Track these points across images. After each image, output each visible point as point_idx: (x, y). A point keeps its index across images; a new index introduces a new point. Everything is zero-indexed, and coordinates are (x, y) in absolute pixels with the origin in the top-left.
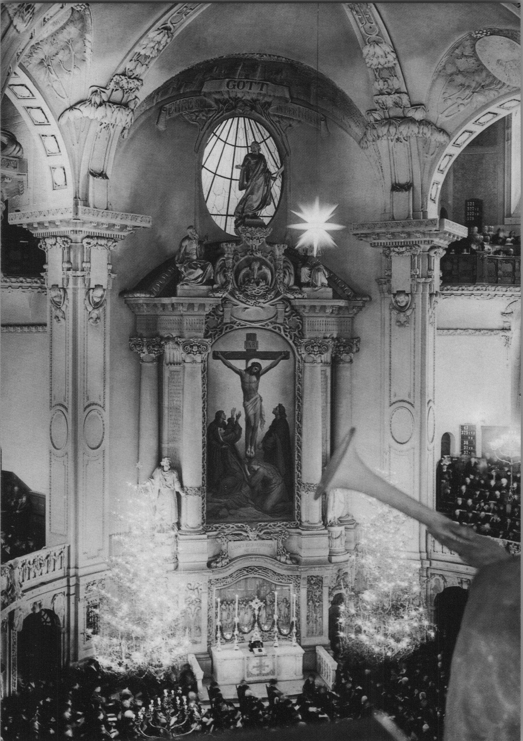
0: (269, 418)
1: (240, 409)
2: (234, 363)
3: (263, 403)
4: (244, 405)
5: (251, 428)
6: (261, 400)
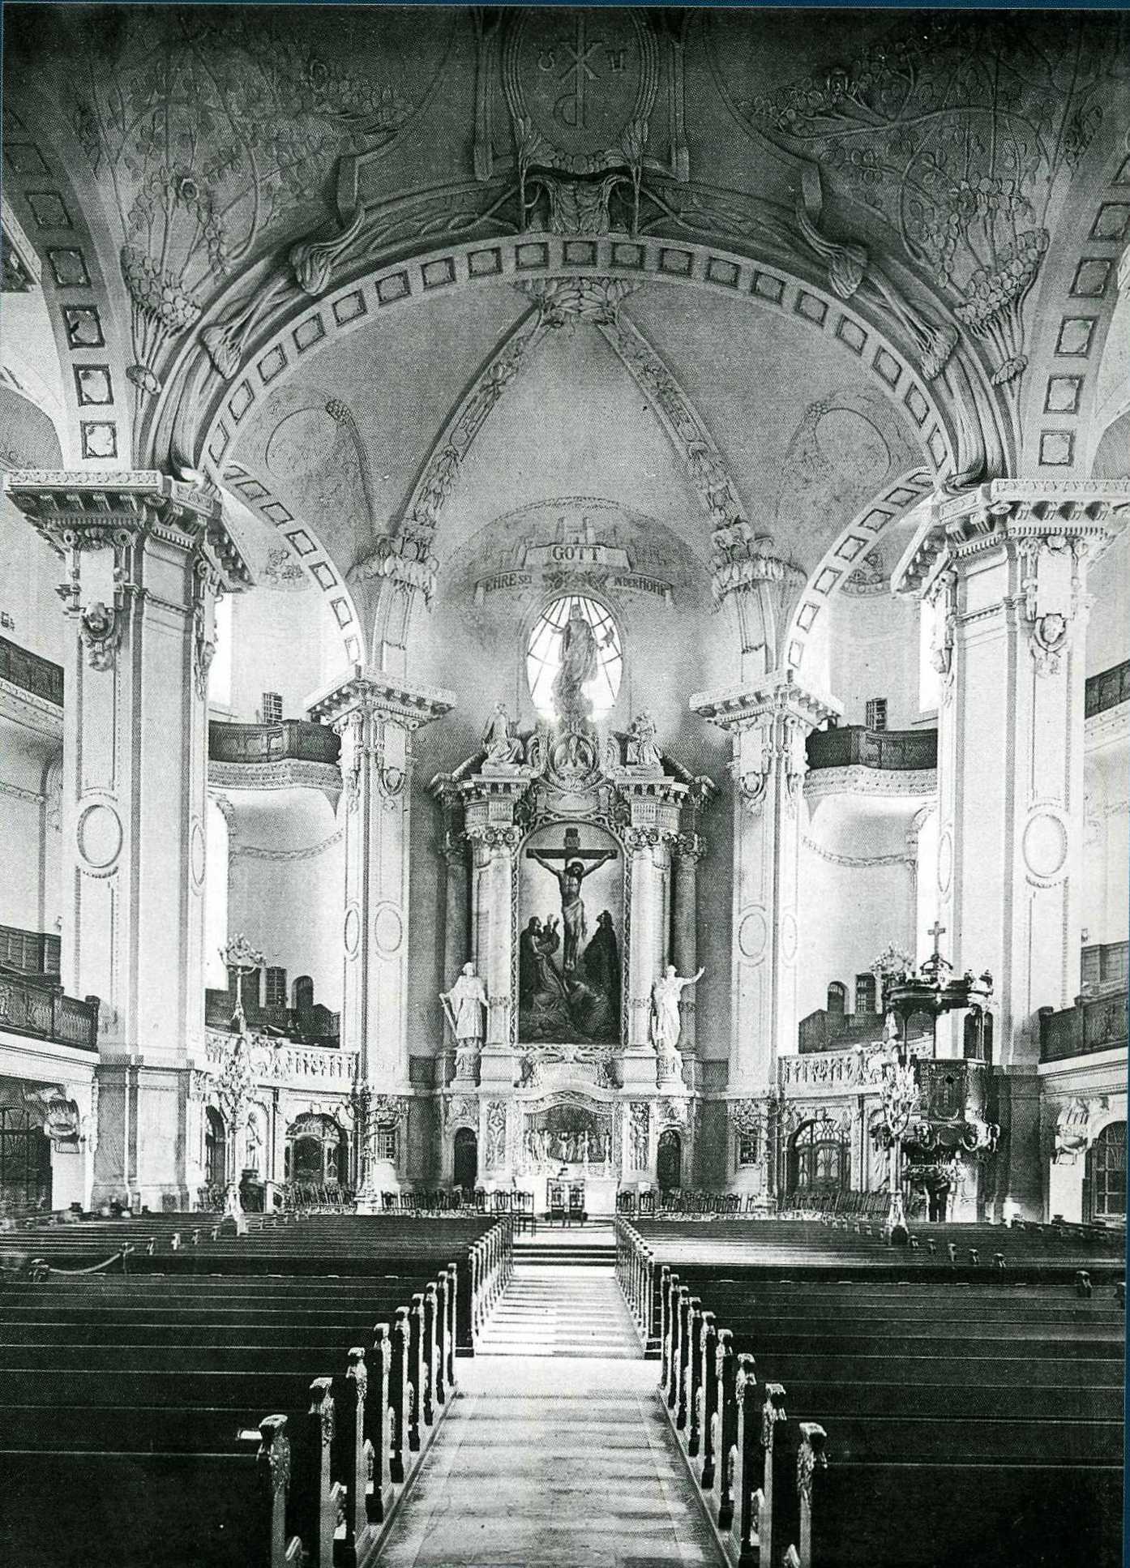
0: (593, 927)
2: (553, 862)
4: (563, 911)
5: (571, 938)
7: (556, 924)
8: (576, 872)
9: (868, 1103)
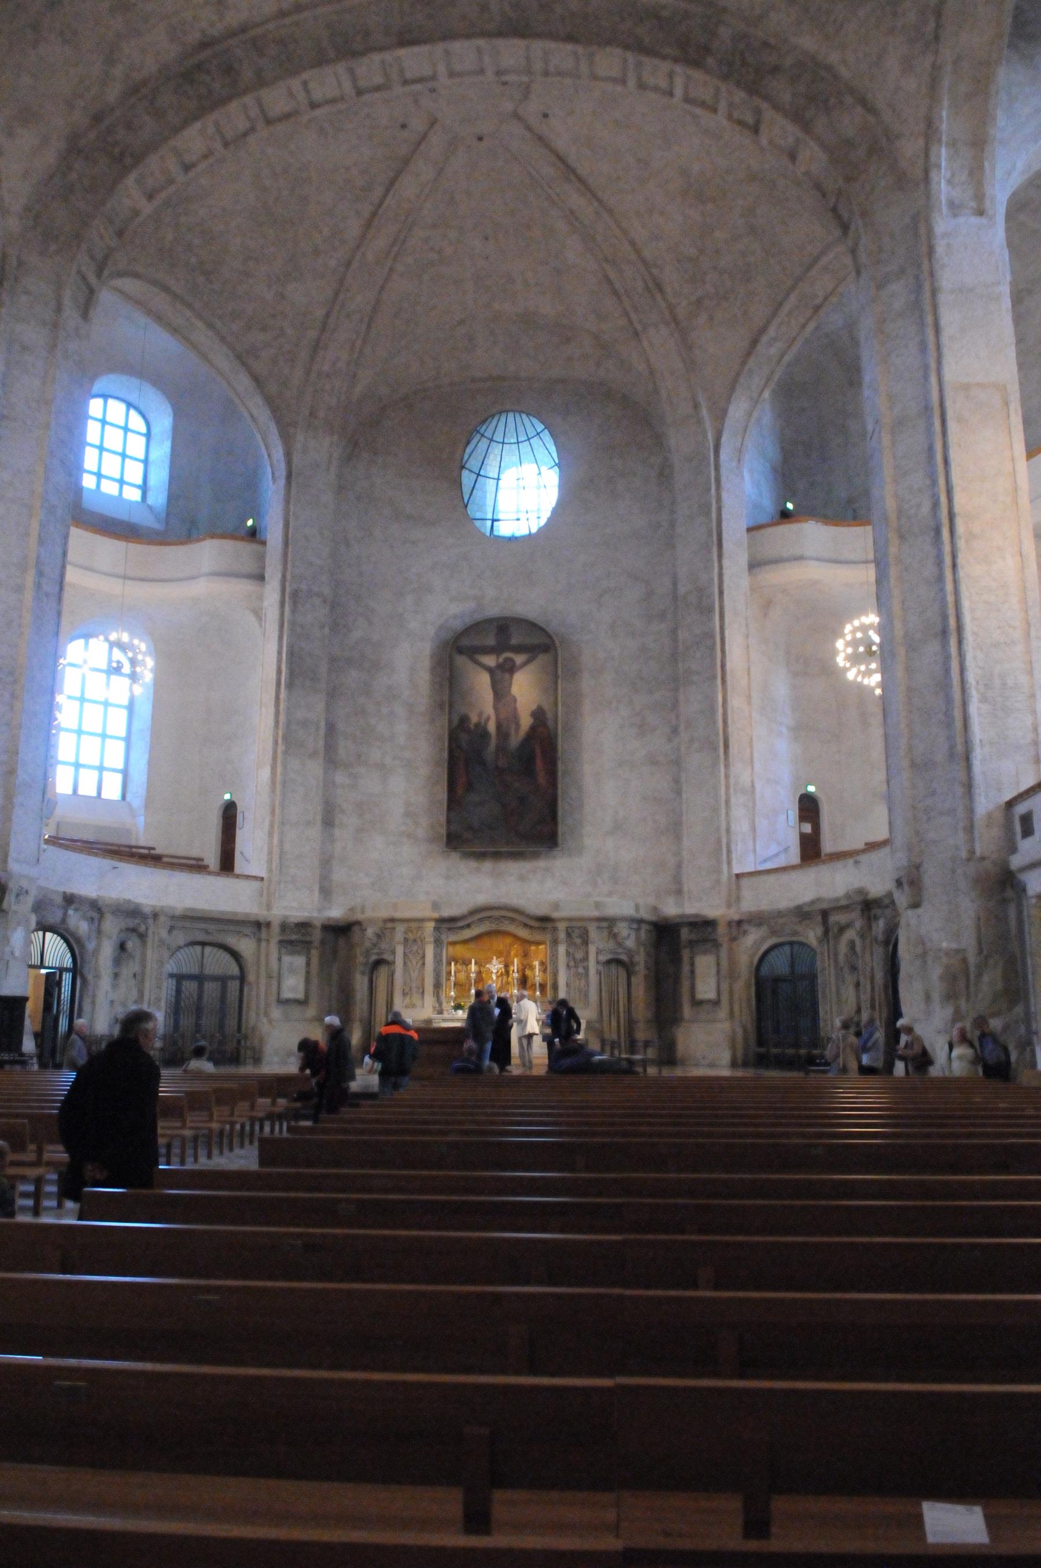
0: (526, 722)
1: (489, 710)
3: (518, 704)
4: (496, 708)
6: (515, 700)
7: (488, 719)
8: (510, 668)
9: (833, 918)
